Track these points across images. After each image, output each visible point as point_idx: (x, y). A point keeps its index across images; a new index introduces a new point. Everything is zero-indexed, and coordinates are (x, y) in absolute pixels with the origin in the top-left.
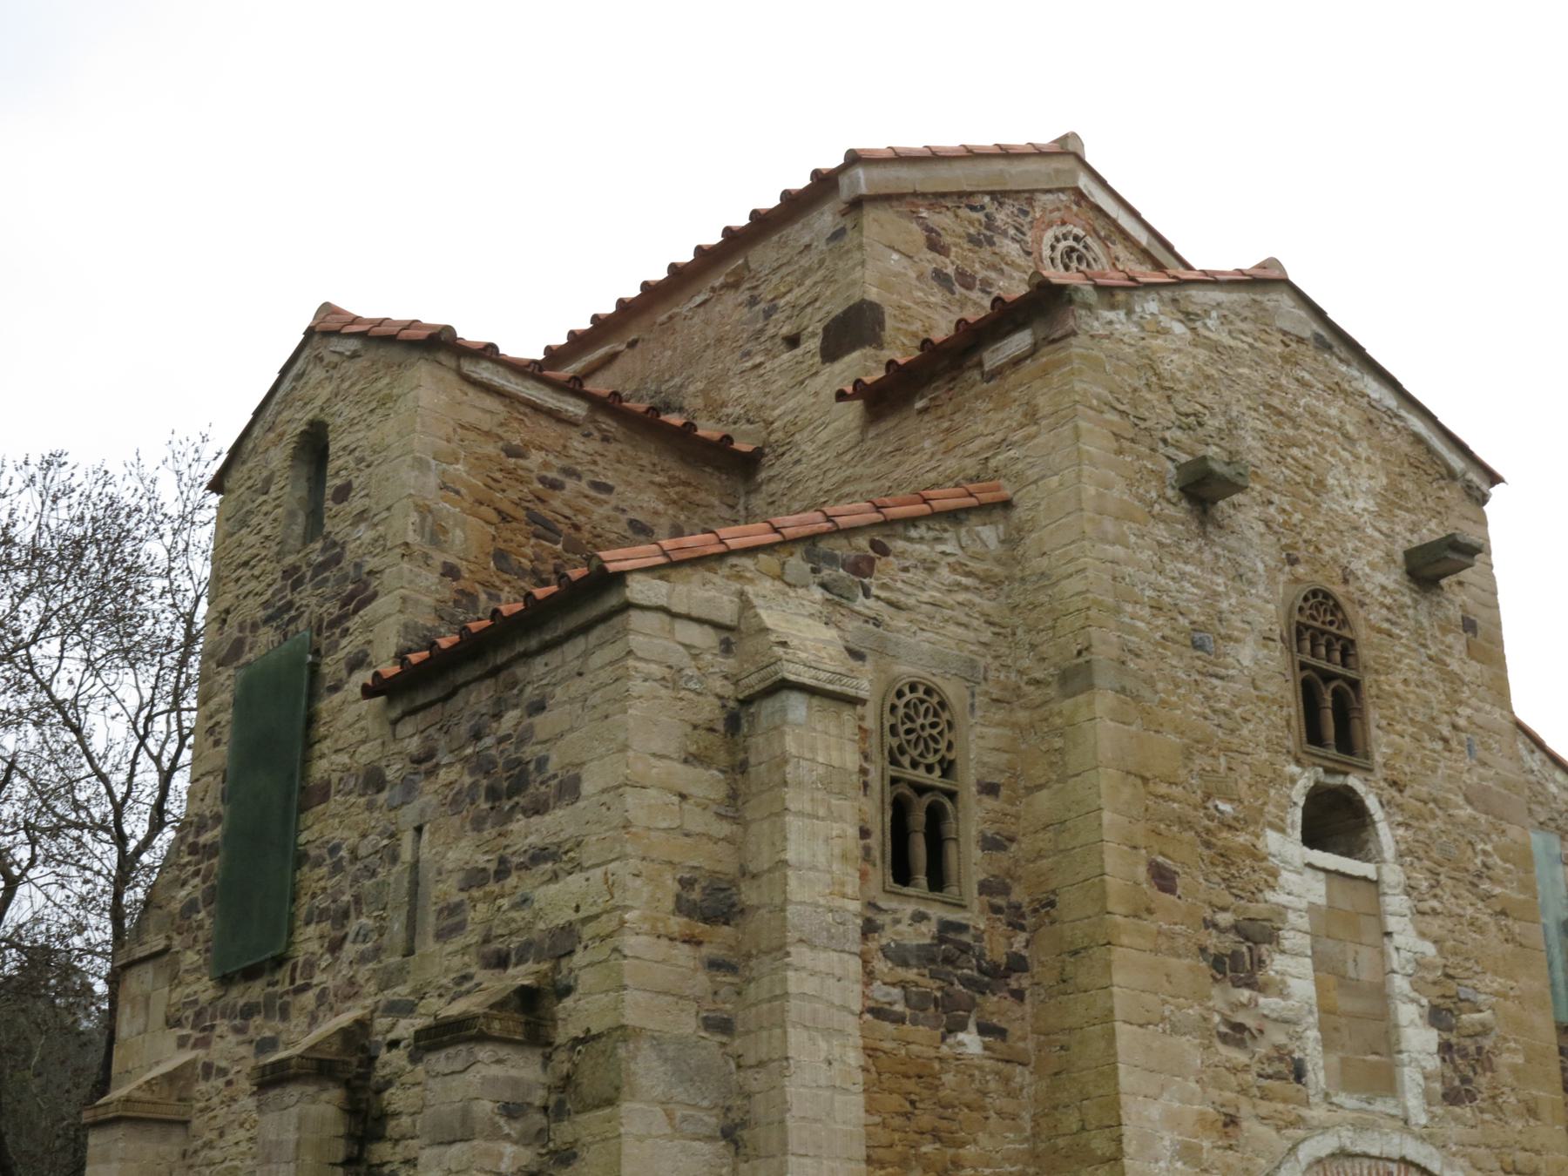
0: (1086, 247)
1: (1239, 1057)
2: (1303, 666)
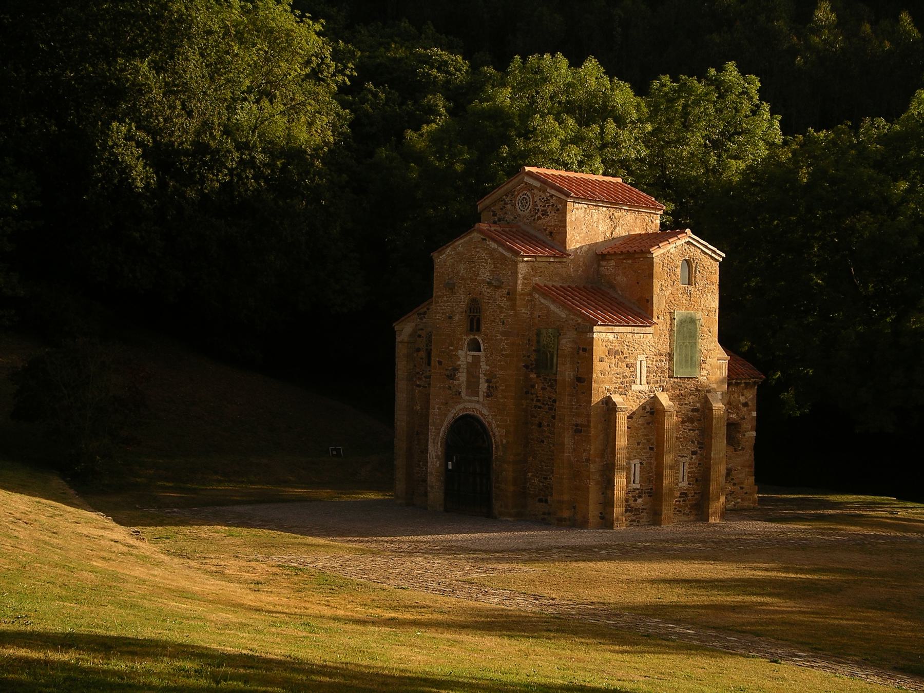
0: (528, 196)
1: (450, 392)
2: (470, 316)
